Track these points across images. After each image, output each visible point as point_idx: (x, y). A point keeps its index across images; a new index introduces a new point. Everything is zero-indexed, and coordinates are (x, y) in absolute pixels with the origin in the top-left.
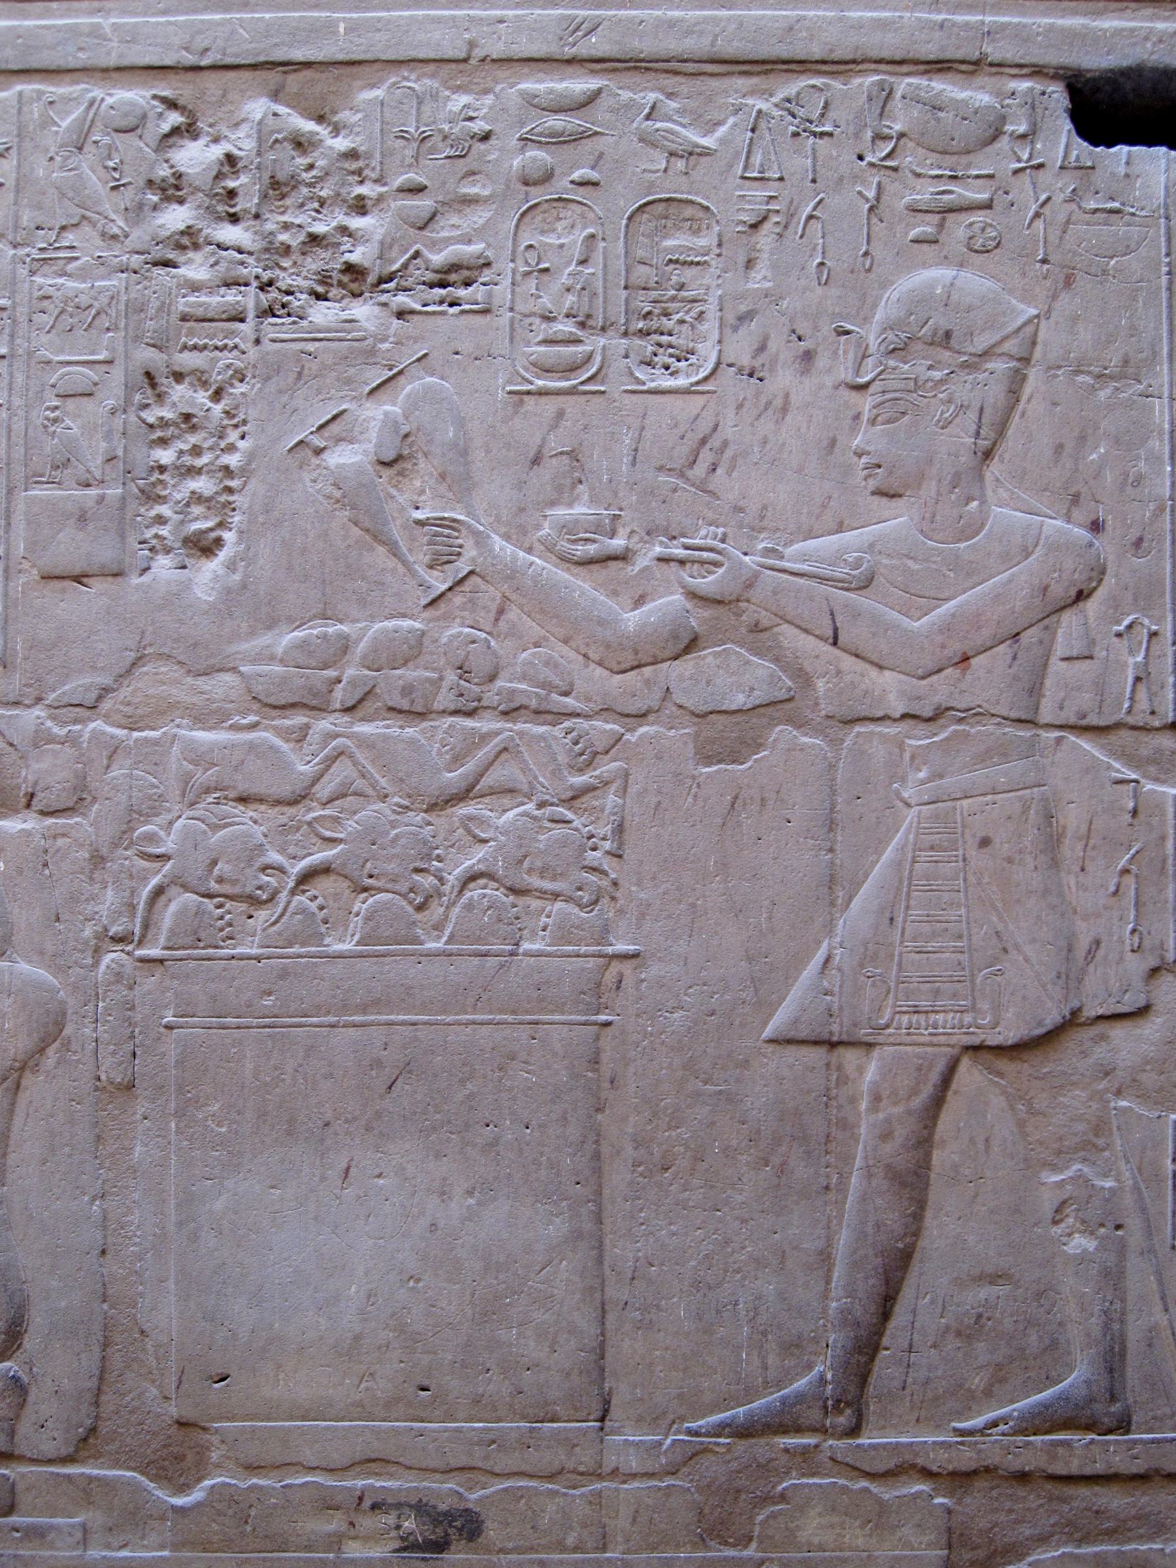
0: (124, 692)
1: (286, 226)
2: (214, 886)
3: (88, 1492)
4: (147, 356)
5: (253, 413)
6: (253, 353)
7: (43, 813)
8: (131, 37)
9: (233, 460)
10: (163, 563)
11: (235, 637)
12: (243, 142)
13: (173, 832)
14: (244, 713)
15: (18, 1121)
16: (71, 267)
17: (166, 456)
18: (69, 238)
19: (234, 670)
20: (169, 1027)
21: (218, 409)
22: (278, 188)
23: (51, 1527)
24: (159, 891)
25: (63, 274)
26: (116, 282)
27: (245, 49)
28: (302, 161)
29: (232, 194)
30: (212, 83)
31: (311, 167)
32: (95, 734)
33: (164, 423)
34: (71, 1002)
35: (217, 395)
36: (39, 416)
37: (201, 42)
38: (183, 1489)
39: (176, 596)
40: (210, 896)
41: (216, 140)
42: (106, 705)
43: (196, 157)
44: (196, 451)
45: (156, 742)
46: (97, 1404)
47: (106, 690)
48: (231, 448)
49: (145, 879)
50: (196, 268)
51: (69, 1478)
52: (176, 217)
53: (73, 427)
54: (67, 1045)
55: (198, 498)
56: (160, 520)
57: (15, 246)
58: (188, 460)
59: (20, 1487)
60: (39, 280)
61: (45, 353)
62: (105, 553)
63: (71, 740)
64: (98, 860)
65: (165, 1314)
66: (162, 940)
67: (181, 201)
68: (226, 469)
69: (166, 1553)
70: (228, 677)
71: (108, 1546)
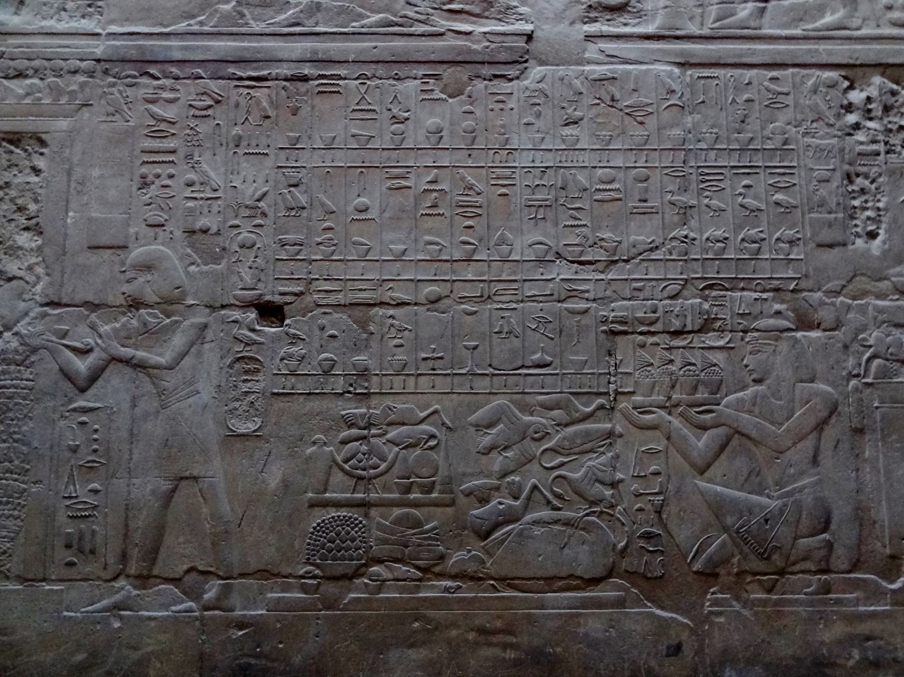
0: (850, 287)
1: (890, 122)
2: (890, 357)
3: (857, 585)
4: (846, 167)
5: (887, 188)
6: (884, 167)
7: (825, 330)
8: (830, 53)
9: (881, 205)
10: (859, 242)
11: (888, 268)
12: (873, 92)
13: (873, 336)
14: (893, 294)
15: (823, 441)
16: (817, 135)
17: (856, 203)
18: (815, 125)
19: (888, 279)
20: (877, 408)
21: (873, 187)
22: (887, 109)
23: (846, 598)
24: (869, 360)
25: (813, 137)
26: (834, 141)
27: (872, 58)
28: (894, 99)
29: (869, 111)
30: (860, 72)
31: (897, 101)
32: (842, 302)
33: (853, 191)
34: (841, 399)
35: (872, 182)
36: (811, 188)
37: (855, 56)
38: (892, 582)
39: (866, 253)
40: (887, 360)
41: (862, 90)
42: (844, 292)
43: (856, 96)
44: (866, 201)
45: (862, 305)
46: (860, 549)
47: (844, 286)
48: (879, 201)
49: (863, 353)
50: (860, 136)
51: (849, 578)
52: (852, 118)
53: (823, 192)
54: (839, 414)
55: (869, 218)
56: (856, 226)
57: (795, 127)
58: (864, 205)
59: (832, 582)
60: (806, 139)
61: (811, 166)
62: (840, 238)
63: (833, 304)
64: (846, 347)
65: (883, 514)
66: (872, 376)
67: (851, 112)
68: (879, 209)
69: (888, 608)
70: (886, 282)
71: (865, 605)
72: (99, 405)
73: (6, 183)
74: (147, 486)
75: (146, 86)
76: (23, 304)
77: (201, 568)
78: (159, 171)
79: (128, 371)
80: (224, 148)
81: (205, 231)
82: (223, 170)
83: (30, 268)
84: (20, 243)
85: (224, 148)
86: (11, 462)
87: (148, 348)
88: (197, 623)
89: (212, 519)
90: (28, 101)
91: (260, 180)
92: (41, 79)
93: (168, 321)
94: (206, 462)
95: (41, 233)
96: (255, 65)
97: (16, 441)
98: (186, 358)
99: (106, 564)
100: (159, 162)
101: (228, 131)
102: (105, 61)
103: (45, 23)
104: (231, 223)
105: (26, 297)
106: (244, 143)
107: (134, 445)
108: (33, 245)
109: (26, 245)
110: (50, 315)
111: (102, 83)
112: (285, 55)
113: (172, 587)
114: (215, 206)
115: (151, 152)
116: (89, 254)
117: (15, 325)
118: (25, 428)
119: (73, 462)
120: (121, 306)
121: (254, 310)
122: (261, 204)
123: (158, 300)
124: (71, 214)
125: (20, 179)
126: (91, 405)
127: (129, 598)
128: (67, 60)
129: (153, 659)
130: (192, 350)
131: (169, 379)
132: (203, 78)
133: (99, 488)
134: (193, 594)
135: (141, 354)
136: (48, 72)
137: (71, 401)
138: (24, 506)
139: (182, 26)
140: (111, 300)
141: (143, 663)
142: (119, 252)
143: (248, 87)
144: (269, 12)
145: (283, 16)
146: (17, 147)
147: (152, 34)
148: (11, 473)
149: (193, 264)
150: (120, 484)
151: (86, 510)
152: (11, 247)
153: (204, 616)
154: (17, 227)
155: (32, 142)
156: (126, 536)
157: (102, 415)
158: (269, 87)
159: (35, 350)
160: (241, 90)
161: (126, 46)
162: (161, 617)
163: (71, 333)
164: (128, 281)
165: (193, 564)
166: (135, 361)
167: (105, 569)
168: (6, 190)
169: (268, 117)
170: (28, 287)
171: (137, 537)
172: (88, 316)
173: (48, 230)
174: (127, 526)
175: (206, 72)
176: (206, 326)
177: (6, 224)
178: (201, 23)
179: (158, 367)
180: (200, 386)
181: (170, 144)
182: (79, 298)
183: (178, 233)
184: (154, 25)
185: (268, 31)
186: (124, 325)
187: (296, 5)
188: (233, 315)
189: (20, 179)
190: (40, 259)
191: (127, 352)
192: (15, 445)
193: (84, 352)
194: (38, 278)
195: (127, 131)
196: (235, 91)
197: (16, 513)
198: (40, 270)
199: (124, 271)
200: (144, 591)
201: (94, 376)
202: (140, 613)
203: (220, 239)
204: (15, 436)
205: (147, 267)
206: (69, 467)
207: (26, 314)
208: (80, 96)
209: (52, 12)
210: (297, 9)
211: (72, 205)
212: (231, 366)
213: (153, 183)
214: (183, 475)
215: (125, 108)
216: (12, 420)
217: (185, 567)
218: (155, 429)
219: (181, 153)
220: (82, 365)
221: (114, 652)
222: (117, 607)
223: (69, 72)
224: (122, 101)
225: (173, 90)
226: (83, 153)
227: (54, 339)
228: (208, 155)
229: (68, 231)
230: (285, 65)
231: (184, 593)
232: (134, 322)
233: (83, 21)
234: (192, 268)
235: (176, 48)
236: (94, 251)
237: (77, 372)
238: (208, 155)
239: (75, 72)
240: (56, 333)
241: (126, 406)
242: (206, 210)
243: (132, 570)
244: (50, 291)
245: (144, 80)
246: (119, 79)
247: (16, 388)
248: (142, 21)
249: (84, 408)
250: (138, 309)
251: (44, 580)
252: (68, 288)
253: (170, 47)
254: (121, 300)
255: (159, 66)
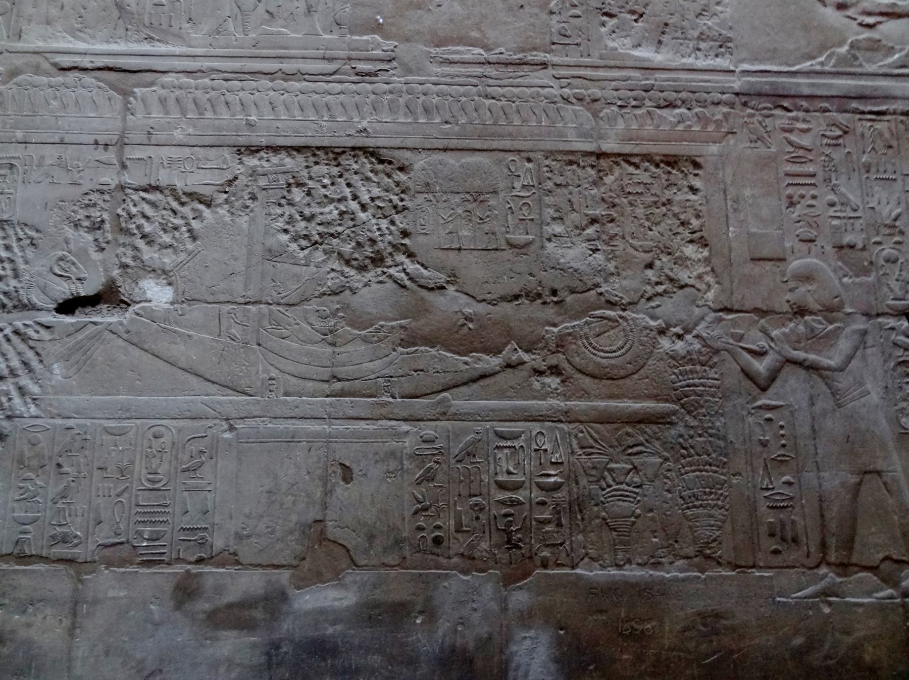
72: (781, 403)
73: (669, 200)
74: (835, 479)
75: (781, 117)
76: (697, 311)
77: (895, 557)
78: (803, 192)
79: (802, 373)
80: (856, 173)
81: (852, 247)
82: (859, 193)
83: (700, 277)
84: (687, 254)
85: (856, 173)
86: (709, 455)
87: (818, 352)
88: (901, 610)
89: (900, 511)
90: (680, 128)
91: (893, 202)
92: (689, 109)
93: (831, 327)
94: (886, 457)
95: (706, 245)
96: (873, 101)
97: (711, 436)
98: (853, 362)
99: (809, 552)
100: (802, 185)
101: (858, 160)
102: (743, 94)
103: (684, 60)
104: (873, 240)
105: (700, 303)
106: (873, 169)
107: (817, 440)
108: (700, 256)
109: (693, 256)
110: (724, 319)
111: (742, 114)
112: (898, 93)
113: (869, 574)
114: (858, 224)
115: (793, 175)
116: (751, 265)
117: (694, 328)
118: (718, 424)
119: (765, 456)
120: (786, 313)
121: (905, 318)
122: (897, 223)
123: (820, 308)
124: (731, 229)
125: (679, 197)
126: (774, 403)
127: (834, 584)
128: (709, 93)
129: (866, 645)
130: (858, 353)
131: (841, 380)
132: (830, 111)
133: (792, 480)
134: (890, 581)
135: (812, 357)
136: (694, 103)
137: (755, 399)
138: (726, 497)
139: (806, 65)
140: (777, 307)
141: (857, 647)
142: (778, 263)
143: (870, 120)
144: (879, 55)
145: (890, 60)
146: (673, 168)
147: (781, 72)
148: (710, 465)
149: (845, 276)
150: (810, 477)
151: (783, 500)
152: (680, 258)
153: (905, 602)
154: (682, 240)
155: (687, 164)
156: (823, 526)
157: (786, 413)
158: (888, 121)
159: (717, 352)
160: (864, 123)
161: (761, 82)
162: (869, 603)
163: (746, 336)
164: (791, 290)
165: (887, 553)
166: (807, 364)
167: (808, 556)
168: (669, 206)
169: (890, 147)
170: (700, 295)
171: (833, 526)
172: (758, 321)
173: (712, 241)
174: (822, 516)
175: (831, 106)
176: (864, 333)
177: (673, 237)
178: (822, 64)
179: (829, 369)
180: (869, 386)
181: (811, 169)
182: (748, 305)
183: (828, 248)
184: (780, 65)
185: (884, 70)
186: (791, 330)
187: (901, 50)
188: (888, 323)
189: (679, 197)
190: (709, 269)
191: (800, 355)
192: (710, 439)
193: (759, 354)
194: (709, 286)
195: (769, 157)
196: (859, 124)
197: (720, 503)
198: (709, 278)
199: (787, 281)
200: (846, 579)
201: (773, 377)
202: (847, 599)
203: (865, 254)
204: (710, 431)
205: (806, 277)
206: (762, 460)
207: (702, 319)
208: (724, 124)
209: (689, 51)
210: (903, 53)
211: (731, 221)
212: (894, 369)
213: (799, 202)
214: (867, 469)
215: (766, 135)
216: (705, 416)
217: (881, 556)
218: (833, 425)
219: (820, 174)
220: (761, 366)
221: (829, 636)
222: (825, 593)
223: (713, 103)
224: (762, 129)
225: (804, 121)
226: (734, 175)
227: (731, 341)
228: (843, 178)
229: (734, 245)
230: (900, 102)
231: (883, 580)
232: (801, 328)
233: (718, 60)
234: (845, 280)
235: (804, 84)
236: (757, 263)
237: (760, 374)
238: (843, 178)
239: (718, 104)
240: (733, 336)
241: (805, 404)
242: (849, 228)
243: (833, 557)
244: (723, 298)
245: (778, 112)
246: (757, 110)
247: (704, 386)
248: (771, 60)
249: (769, 405)
250: (802, 316)
251: (753, 567)
252: (737, 296)
253: (799, 85)
254: (786, 308)
255: (790, 100)
